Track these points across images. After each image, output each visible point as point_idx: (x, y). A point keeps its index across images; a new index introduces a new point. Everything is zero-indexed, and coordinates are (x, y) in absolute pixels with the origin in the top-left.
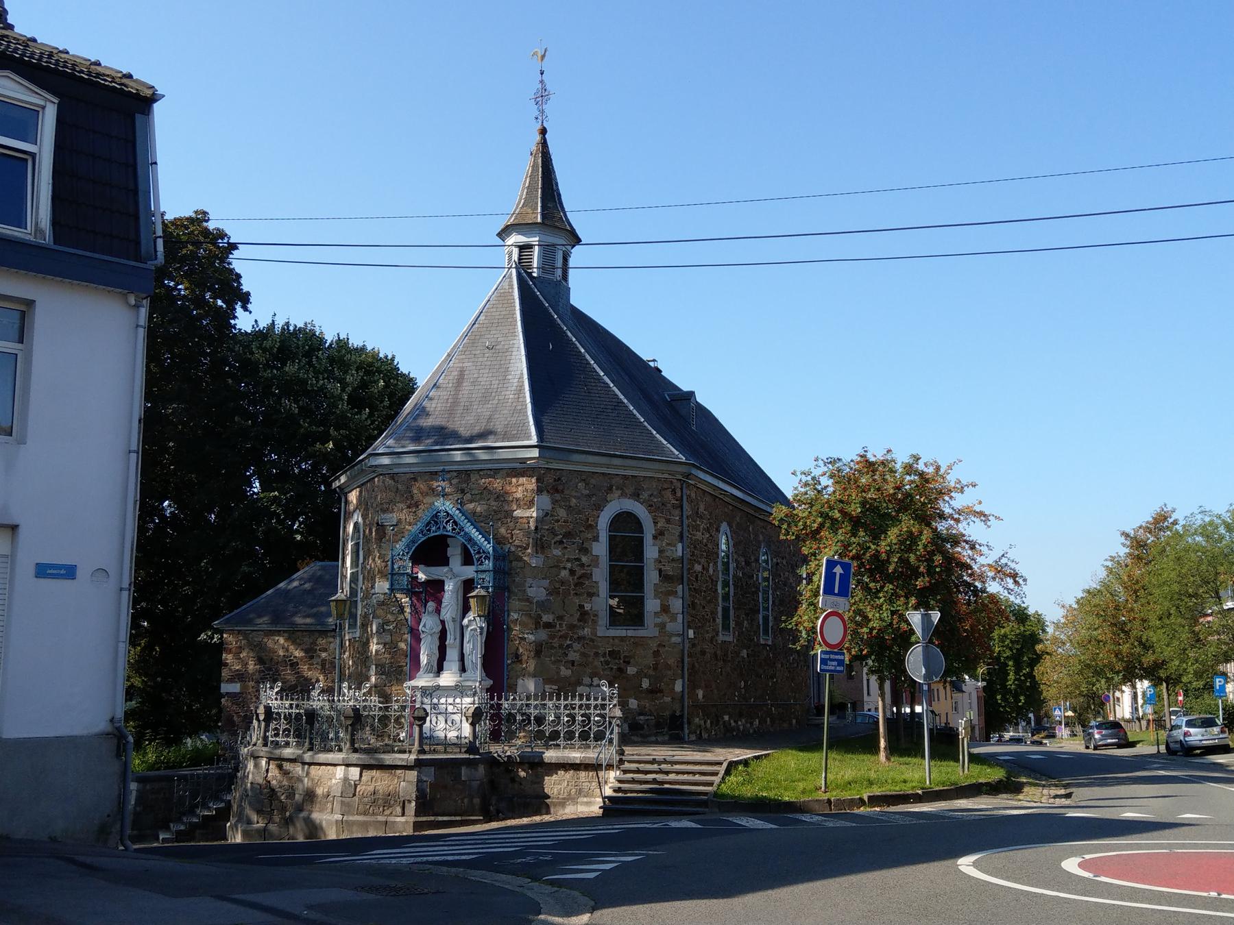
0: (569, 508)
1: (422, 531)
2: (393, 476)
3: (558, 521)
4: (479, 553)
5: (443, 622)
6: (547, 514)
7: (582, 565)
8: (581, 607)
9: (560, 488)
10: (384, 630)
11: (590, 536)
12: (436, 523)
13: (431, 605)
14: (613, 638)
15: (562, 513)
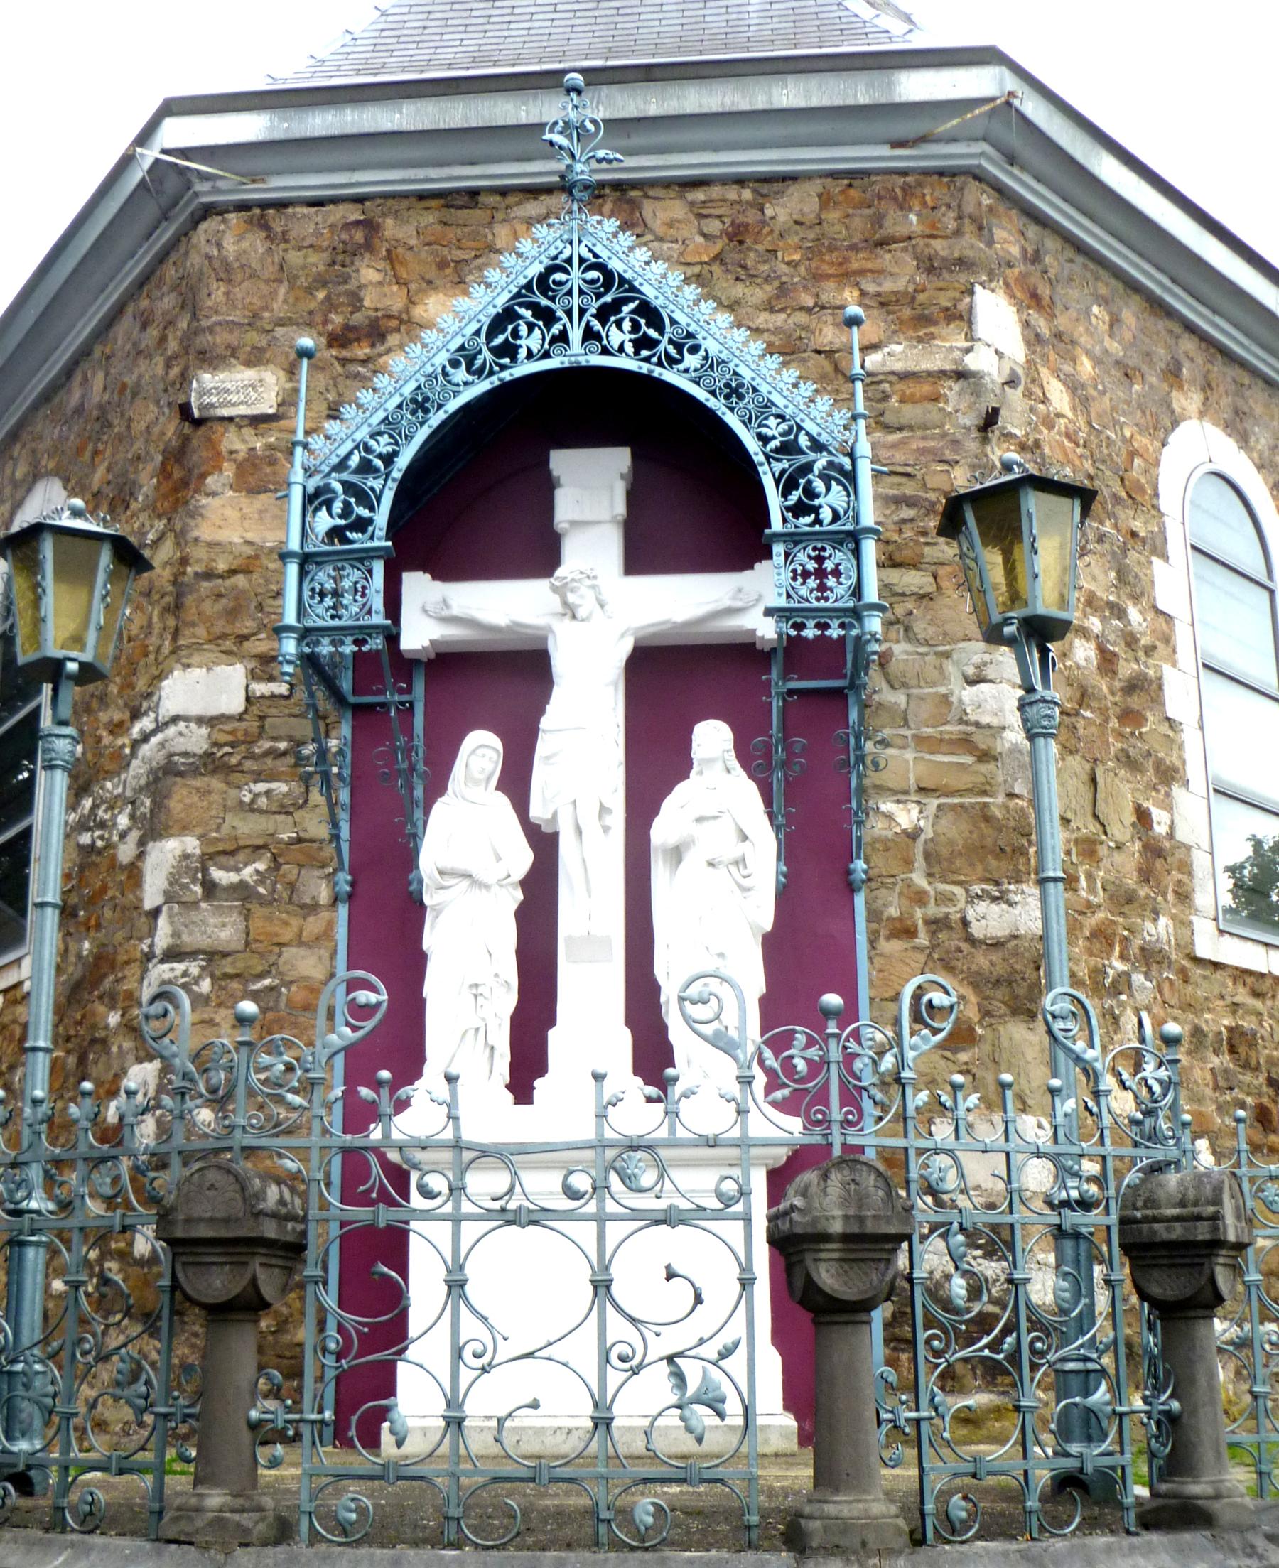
0: (1074, 387)
1: (465, 357)
2: (261, 213)
3: (1049, 422)
4: (789, 448)
5: (544, 844)
6: (1012, 382)
7: (1131, 640)
8: (1143, 817)
9: (1044, 291)
10: (210, 888)
11: (1137, 525)
12: (548, 317)
13: (480, 751)
14: (1242, 974)
15: (1059, 398)
